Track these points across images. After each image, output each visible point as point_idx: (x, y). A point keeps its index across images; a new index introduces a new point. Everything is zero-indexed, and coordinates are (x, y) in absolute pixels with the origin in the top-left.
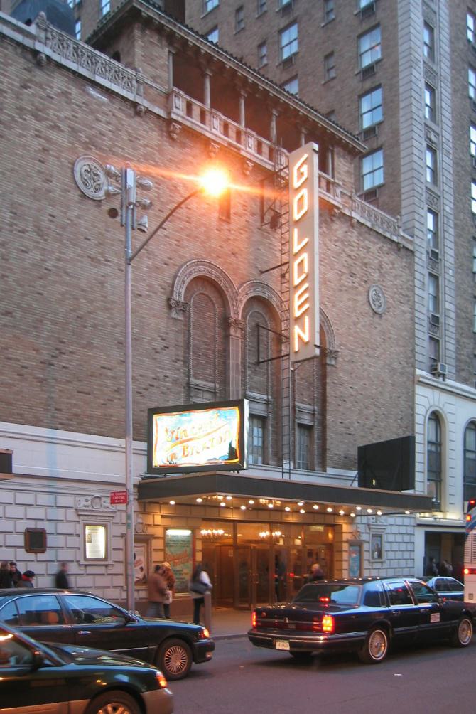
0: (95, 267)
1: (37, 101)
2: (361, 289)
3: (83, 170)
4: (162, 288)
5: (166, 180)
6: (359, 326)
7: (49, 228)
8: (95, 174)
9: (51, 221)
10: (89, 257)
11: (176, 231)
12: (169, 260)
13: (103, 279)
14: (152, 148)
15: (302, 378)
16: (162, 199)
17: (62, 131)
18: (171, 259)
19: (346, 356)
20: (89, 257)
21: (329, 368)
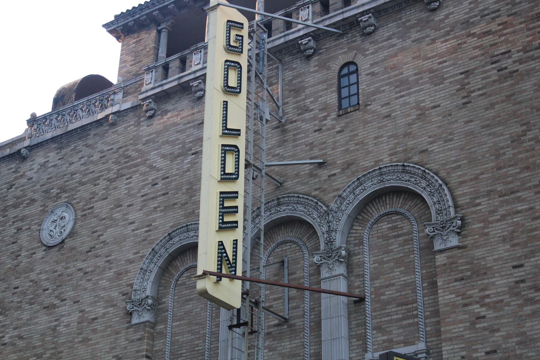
0: (51, 314)
1: (18, 193)
2: (521, 67)
3: (50, 223)
4: (123, 295)
5: (138, 168)
6: (530, 135)
7: (12, 302)
8: (62, 218)
9: (14, 294)
10: (45, 308)
11: (148, 215)
12: (135, 256)
13: (56, 323)
14: (126, 146)
15: (388, 303)
16: (132, 192)
17: (37, 201)
18: (136, 253)
19: (493, 212)
20: (45, 308)
21: (440, 259)
